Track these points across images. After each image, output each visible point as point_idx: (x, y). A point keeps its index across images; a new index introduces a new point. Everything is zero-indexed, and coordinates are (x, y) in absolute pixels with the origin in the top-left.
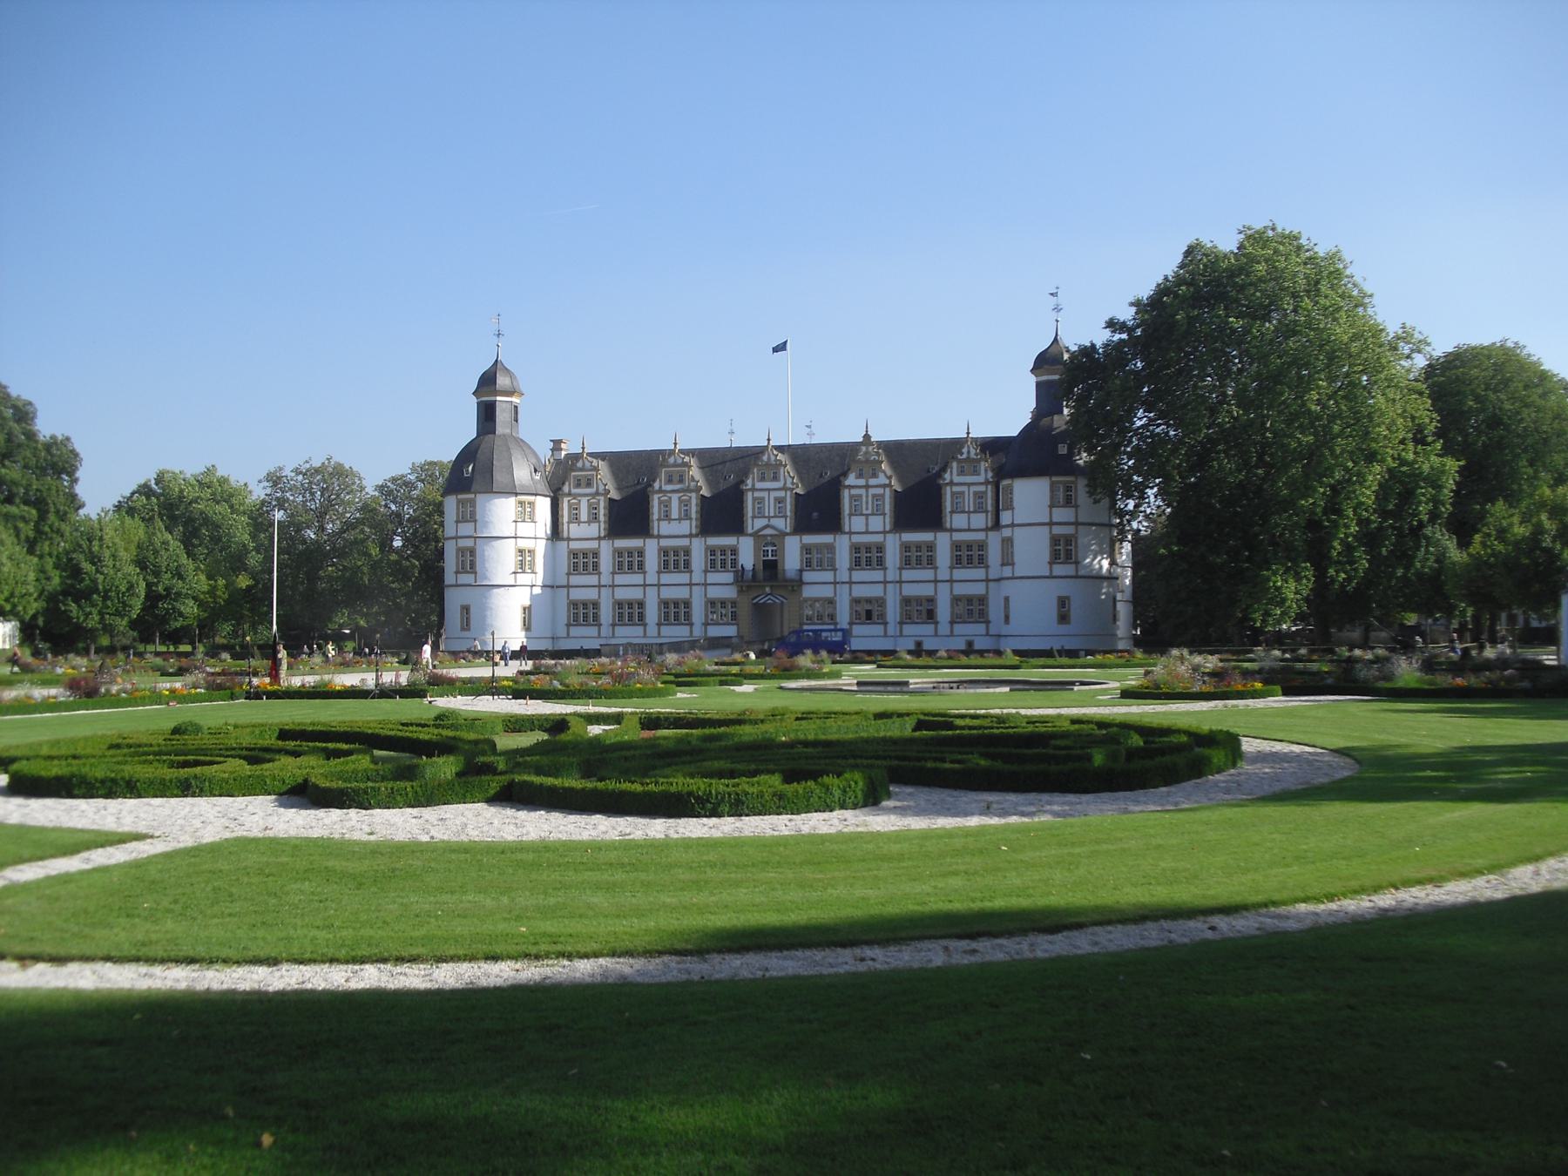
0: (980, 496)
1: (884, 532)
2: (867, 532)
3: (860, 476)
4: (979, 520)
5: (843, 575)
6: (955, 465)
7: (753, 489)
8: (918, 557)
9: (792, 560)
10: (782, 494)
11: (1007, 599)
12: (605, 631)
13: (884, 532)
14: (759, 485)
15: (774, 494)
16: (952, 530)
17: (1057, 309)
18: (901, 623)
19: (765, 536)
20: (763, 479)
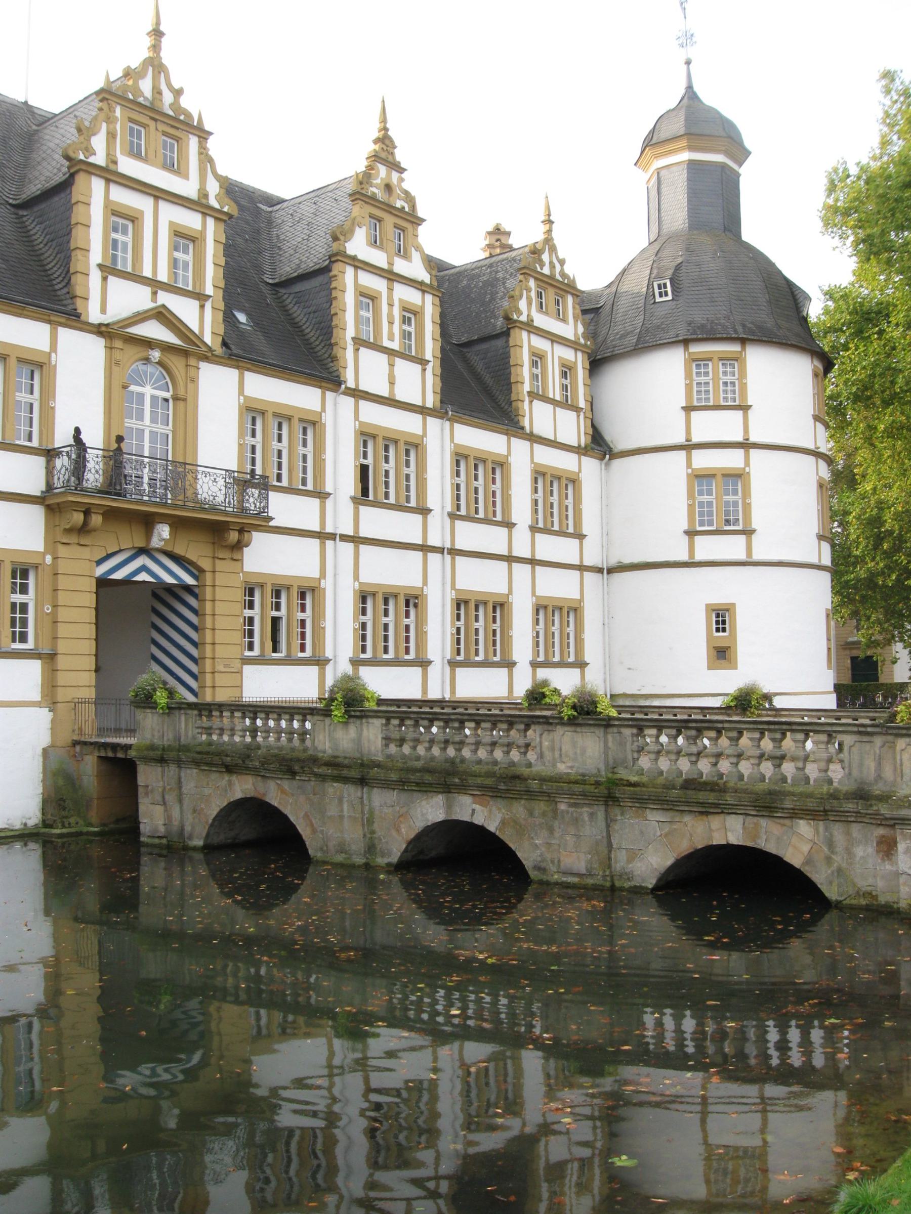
0: (567, 370)
1: (422, 410)
2: (390, 402)
3: (374, 243)
4: (570, 428)
5: (341, 517)
6: (532, 283)
7: (111, 175)
8: (480, 491)
9: (218, 446)
10: (191, 220)
11: (721, 617)
12: (437, 672)
13: (422, 410)
14: (128, 166)
15: (171, 214)
16: (534, 439)
17: (687, 39)
18: (453, 664)
19: (149, 343)
20: (135, 153)
